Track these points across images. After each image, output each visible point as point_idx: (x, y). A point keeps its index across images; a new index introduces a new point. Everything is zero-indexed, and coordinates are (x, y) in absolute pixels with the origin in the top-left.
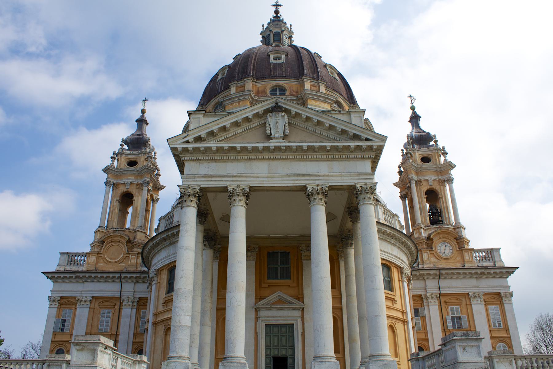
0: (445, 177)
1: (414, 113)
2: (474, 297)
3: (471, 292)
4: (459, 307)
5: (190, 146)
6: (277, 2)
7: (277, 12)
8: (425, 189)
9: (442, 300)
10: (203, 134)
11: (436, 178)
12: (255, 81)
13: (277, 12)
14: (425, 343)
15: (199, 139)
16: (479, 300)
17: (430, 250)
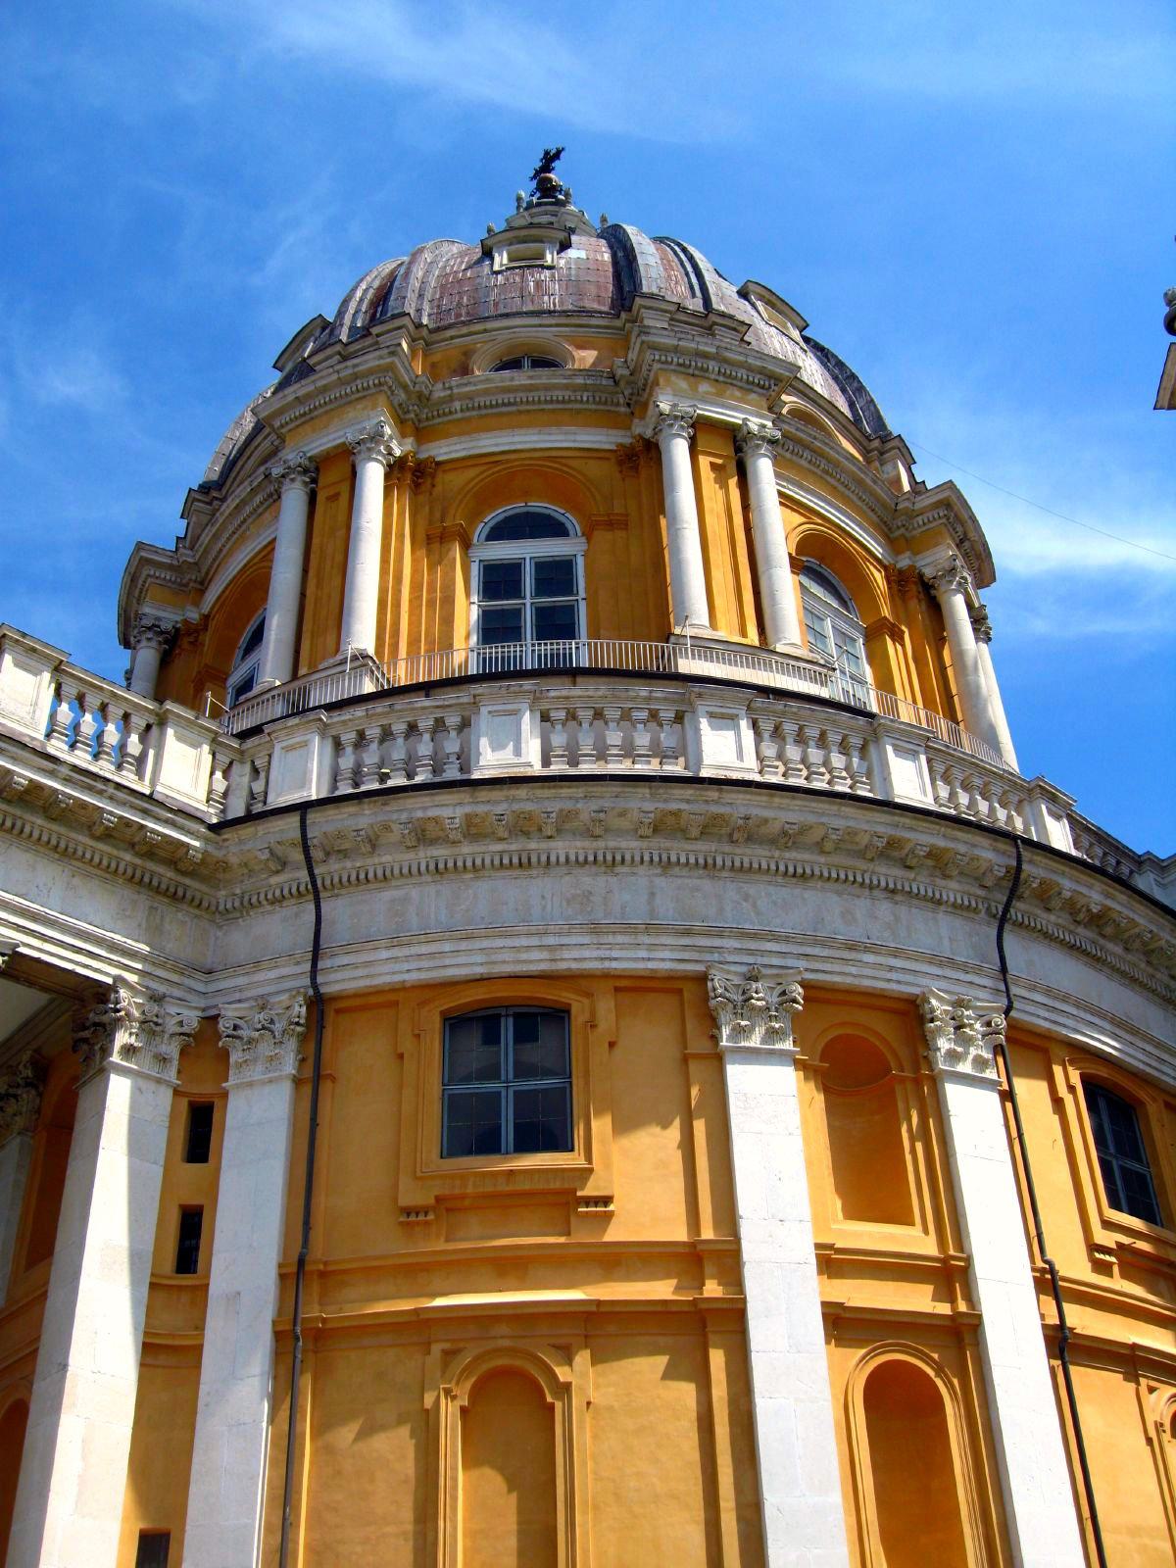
6: (547, 153)
12: (217, 499)
13: (546, 189)
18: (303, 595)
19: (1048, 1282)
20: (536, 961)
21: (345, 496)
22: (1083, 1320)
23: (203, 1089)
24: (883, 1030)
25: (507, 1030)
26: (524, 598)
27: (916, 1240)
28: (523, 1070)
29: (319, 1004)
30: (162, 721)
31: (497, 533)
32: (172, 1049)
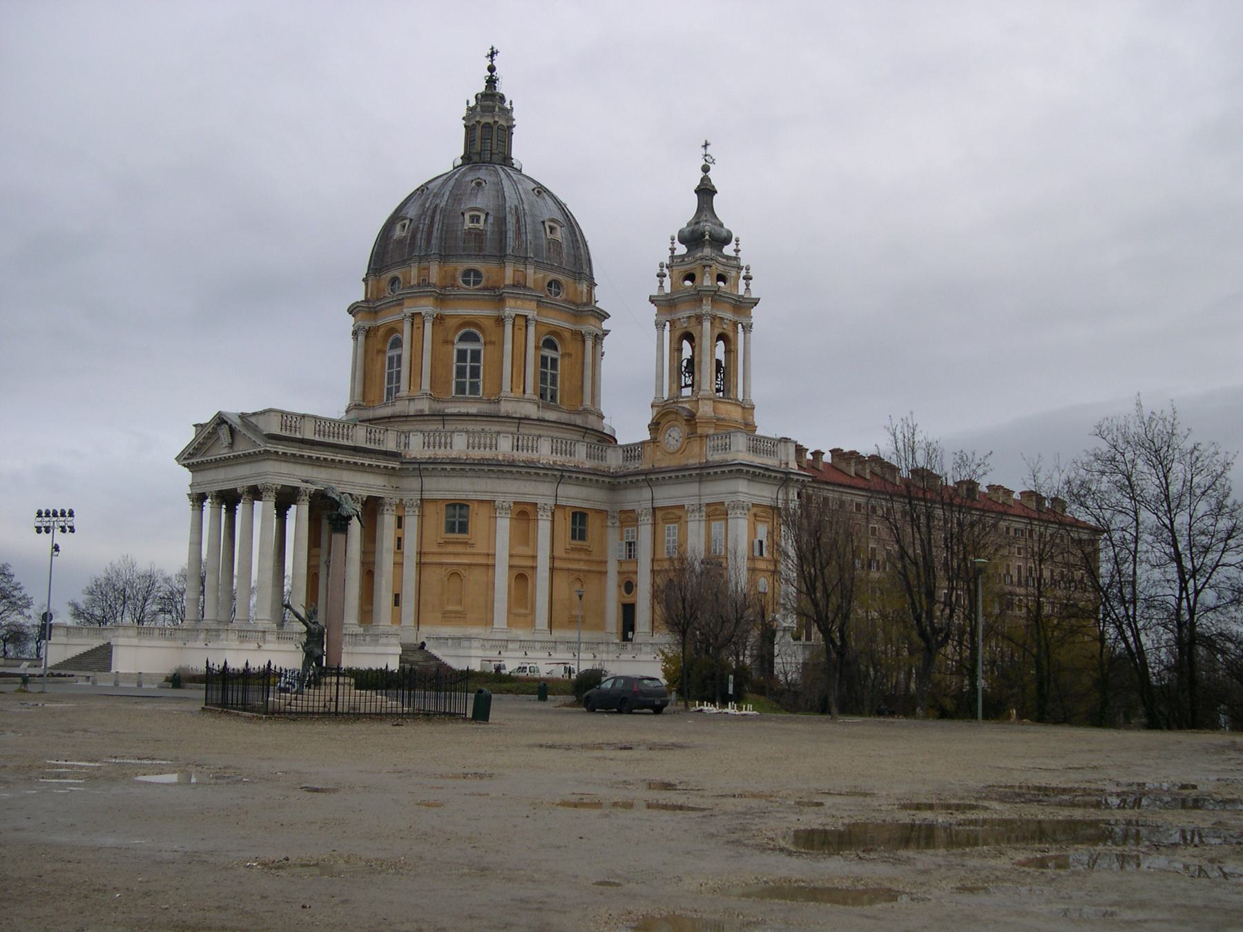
0: (698, 311)
1: (706, 180)
2: (693, 511)
3: (686, 502)
4: (676, 525)
5: (186, 462)
6: (492, 48)
7: (492, 69)
8: (678, 333)
9: (659, 514)
10: (191, 450)
11: (692, 313)
13: (492, 69)
14: (634, 577)
15: (191, 455)
16: (697, 514)
17: (654, 442)
18: (411, 361)
19: (553, 558)
20: (464, 497)
21: (422, 329)
22: (557, 564)
23: (400, 514)
24: (529, 508)
25: (458, 507)
26: (465, 378)
27: (527, 551)
28: (460, 516)
29: (422, 500)
30: (387, 430)
31: (462, 339)
32: (394, 508)
